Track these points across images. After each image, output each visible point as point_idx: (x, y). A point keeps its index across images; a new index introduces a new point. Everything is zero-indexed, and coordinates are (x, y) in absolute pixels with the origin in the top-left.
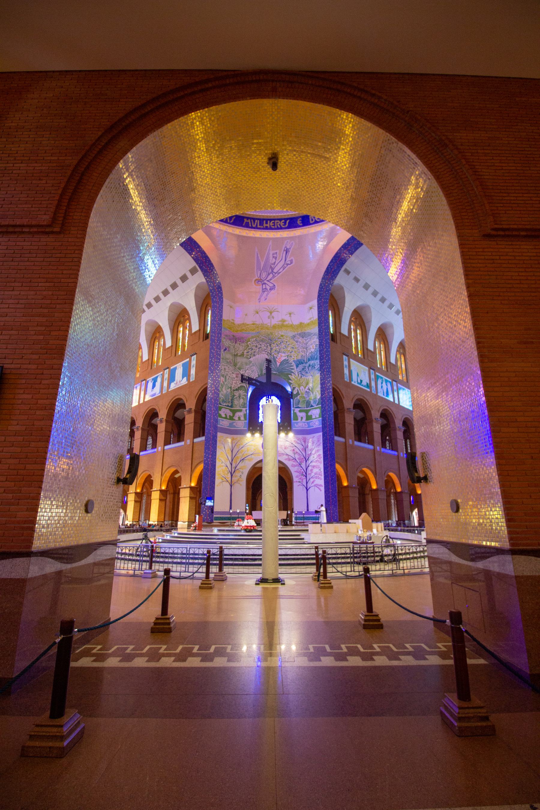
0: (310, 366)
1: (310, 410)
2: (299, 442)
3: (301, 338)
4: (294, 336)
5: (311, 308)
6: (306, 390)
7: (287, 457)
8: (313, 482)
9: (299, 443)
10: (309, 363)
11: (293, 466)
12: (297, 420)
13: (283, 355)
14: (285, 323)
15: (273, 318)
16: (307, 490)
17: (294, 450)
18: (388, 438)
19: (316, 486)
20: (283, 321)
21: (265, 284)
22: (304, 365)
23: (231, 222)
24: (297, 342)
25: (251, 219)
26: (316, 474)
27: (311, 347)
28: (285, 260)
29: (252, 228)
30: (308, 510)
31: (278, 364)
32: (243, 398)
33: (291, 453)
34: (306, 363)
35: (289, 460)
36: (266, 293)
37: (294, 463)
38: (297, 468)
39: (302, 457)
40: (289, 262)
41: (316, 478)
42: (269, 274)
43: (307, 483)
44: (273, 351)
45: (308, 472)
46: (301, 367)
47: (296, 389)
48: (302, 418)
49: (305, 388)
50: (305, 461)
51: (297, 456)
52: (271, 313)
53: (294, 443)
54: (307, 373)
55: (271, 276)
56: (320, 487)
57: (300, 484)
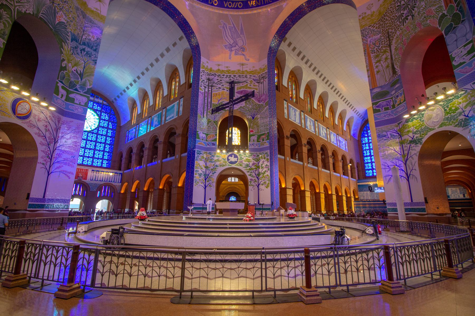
0: (84, 50)
1: (73, 93)
2: (53, 119)
4: (77, 9)
7: (38, 131)
8: (58, 168)
9: (53, 121)
10: (84, 47)
11: (42, 144)
12: (58, 95)
13: (64, 17)
16: (49, 175)
17: (46, 126)
18: (168, 152)
19: (64, 172)
22: (78, 44)
24: (78, 17)
26: (65, 159)
27: (91, 34)
30: (44, 197)
32: (4, 23)
33: (43, 129)
35: (39, 136)
37: (44, 142)
38: (44, 147)
39: (53, 137)
41: (65, 164)
43: (50, 167)
45: (54, 155)
46: (74, 44)
47: (65, 62)
48: (62, 96)
49: (72, 68)
50: (54, 142)
51: (48, 135)
53: (49, 119)
54: (78, 53)
56: (69, 175)
57: (42, 166)
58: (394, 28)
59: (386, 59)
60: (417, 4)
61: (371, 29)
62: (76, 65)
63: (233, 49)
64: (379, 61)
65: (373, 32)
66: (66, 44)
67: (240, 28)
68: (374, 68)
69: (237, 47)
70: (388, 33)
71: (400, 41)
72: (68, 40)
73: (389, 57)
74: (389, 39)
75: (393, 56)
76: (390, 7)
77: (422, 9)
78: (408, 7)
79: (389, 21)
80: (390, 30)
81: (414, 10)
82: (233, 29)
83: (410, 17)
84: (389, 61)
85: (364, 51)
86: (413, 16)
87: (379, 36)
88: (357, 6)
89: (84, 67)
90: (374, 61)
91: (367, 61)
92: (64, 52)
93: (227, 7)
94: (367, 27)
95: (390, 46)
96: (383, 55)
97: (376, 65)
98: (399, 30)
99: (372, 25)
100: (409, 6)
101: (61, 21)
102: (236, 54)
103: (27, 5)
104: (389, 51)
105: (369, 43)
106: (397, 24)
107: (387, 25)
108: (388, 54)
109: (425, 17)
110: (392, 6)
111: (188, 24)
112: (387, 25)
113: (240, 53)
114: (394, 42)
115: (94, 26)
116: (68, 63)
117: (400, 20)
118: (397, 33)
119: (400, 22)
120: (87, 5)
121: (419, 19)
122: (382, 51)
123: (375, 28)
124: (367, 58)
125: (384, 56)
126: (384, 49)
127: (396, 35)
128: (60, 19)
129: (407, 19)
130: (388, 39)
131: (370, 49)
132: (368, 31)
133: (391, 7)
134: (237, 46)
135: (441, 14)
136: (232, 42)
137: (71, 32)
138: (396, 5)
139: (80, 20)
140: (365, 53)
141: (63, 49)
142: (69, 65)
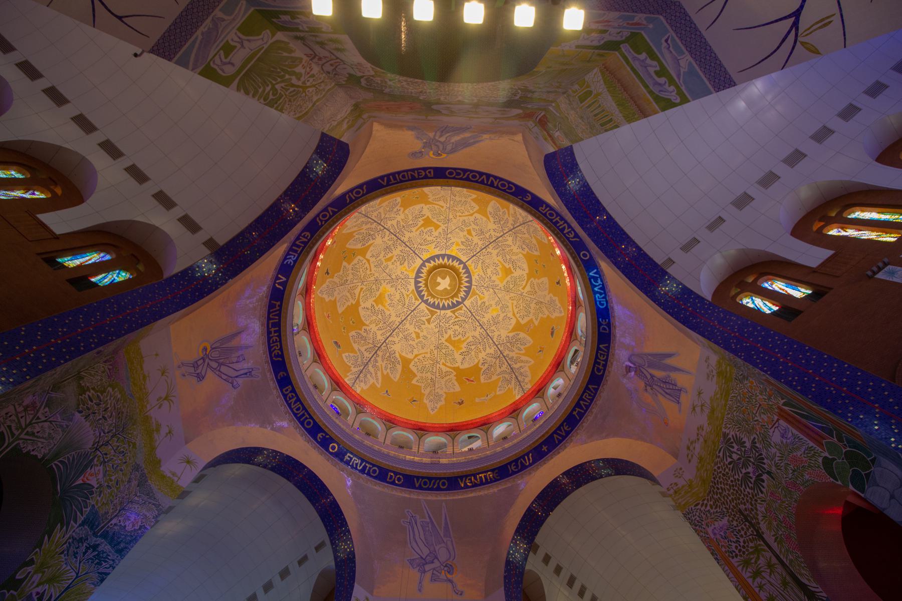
0: (95, 547)
3: (136, 483)
4: (137, 468)
5: (188, 462)
6: (34, 592)
10: (99, 540)
13: (101, 476)
14: (155, 432)
15: (160, 407)
20: (158, 431)
21: (204, 362)
23: (277, 285)
24: (129, 482)
25: (280, 310)
28: (237, 377)
29: (269, 313)
31: (79, 482)
34: (95, 534)
36: (192, 370)
40: (235, 383)
42: (216, 361)
44: (104, 450)
47: (29, 569)
49: (37, 586)
52: (166, 398)
55: (214, 365)
58: (747, 501)
59: (770, 566)
60: (764, 454)
61: (702, 509)
62: (51, 580)
63: (427, 567)
64: (757, 574)
65: (709, 515)
66: (65, 528)
67: (443, 525)
68: (757, 590)
69: (437, 564)
70: (740, 511)
71: (775, 523)
72: (76, 522)
73: (774, 560)
74: (750, 523)
75: (782, 557)
76: (716, 468)
77: (777, 458)
78: (750, 461)
79: (729, 491)
80: (742, 507)
81: (764, 464)
82: (430, 524)
83: (765, 477)
84: (779, 569)
85: (712, 554)
86: (769, 473)
87: (725, 521)
88: (656, 474)
89: (68, 588)
90: (746, 575)
91: (731, 575)
92: (46, 546)
93: (420, 488)
94: (693, 506)
95: (760, 536)
96: (758, 558)
97: (756, 584)
98: (759, 502)
99: (701, 503)
100: (752, 460)
101: (88, 482)
102: (434, 579)
103: (42, 443)
104: (766, 548)
105: (712, 536)
106: (748, 493)
107: (730, 498)
108: (769, 554)
109: (794, 471)
110: (719, 465)
111: (342, 514)
112: (730, 498)
113: (443, 576)
114: (763, 526)
115: (150, 503)
116: (35, 572)
117: (750, 485)
118: (759, 508)
119: (751, 488)
120: (160, 466)
121: (785, 476)
122: (751, 550)
123: (708, 508)
124: (726, 568)
125: (762, 562)
126: (751, 545)
127: (759, 512)
128: (90, 478)
129: (763, 481)
130: (747, 523)
131: (723, 549)
132: (697, 514)
133: (719, 468)
134: (436, 561)
135: (820, 460)
136: (426, 551)
137: (93, 506)
138: (727, 463)
139: (129, 488)
140: (716, 559)
141: (49, 538)
142: (35, 576)
